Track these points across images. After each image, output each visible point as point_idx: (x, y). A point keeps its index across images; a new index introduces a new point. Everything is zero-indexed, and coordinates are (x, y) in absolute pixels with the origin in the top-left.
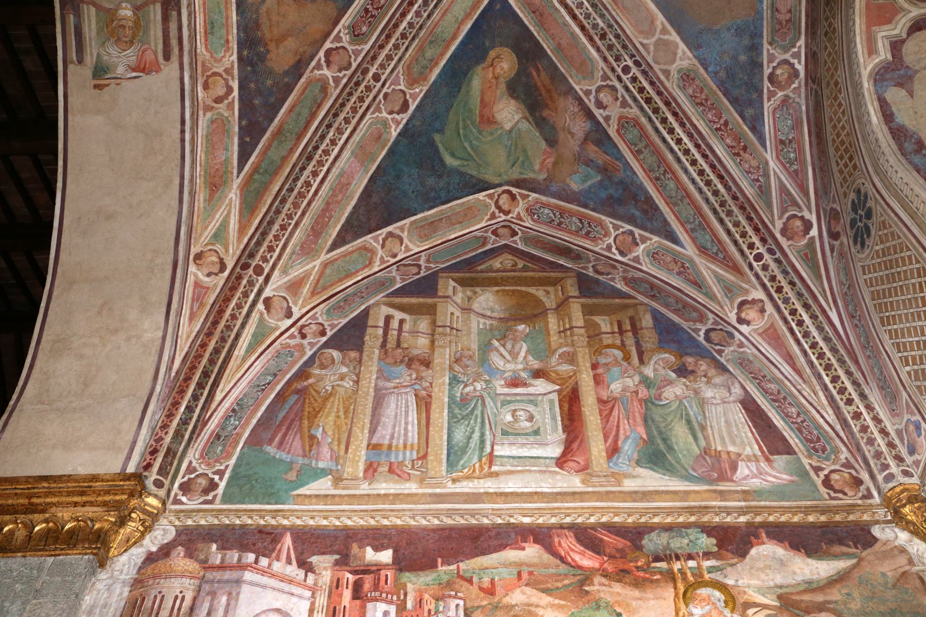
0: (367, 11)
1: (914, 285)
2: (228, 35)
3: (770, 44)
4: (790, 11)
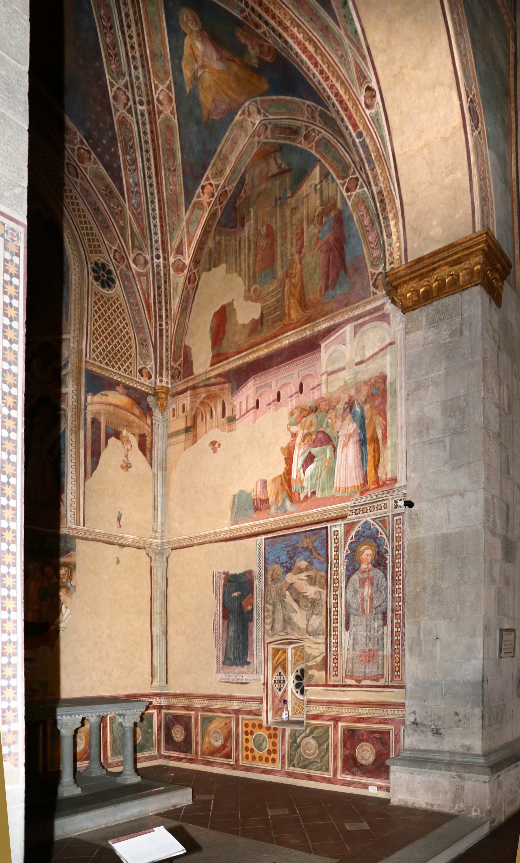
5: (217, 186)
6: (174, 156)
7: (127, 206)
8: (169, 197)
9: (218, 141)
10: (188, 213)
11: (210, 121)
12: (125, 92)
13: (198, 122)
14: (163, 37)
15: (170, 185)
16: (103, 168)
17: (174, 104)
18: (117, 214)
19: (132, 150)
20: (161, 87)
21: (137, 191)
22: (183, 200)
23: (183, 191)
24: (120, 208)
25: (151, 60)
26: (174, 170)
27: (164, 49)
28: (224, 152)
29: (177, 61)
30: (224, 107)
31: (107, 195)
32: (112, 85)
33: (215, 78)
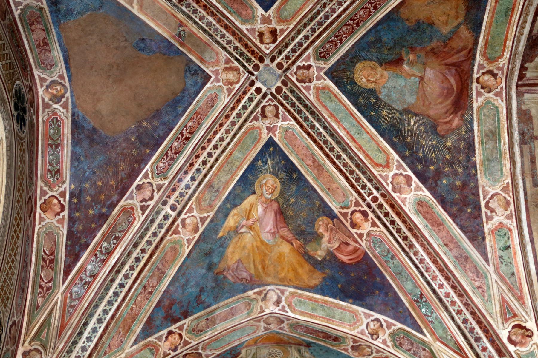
0: (375, 8)
2: (495, 6)
3: (42, 8)
4: (33, 31)
5: (186, 343)
6: (160, 280)
7: (62, 288)
8: (125, 314)
9: (217, 299)
10: (134, 347)
11: (222, 276)
12: (153, 191)
13: (210, 268)
14: (231, 180)
15: (135, 304)
16: (65, 232)
17: (197, 236)
18: (41, 287)
19: (115, 241)
20: (195, 213)
21: (89, 282)
22: (139, 330)
23: (145, 320)
24: (50, 285)
25: (204, 187)
26: (151, 293)
27: (224, 188)
28: (215, 314)
29: (228, 206)
30: (245, 275)
31: (44, 260)
32: (146, 176)
33: (255, 244)
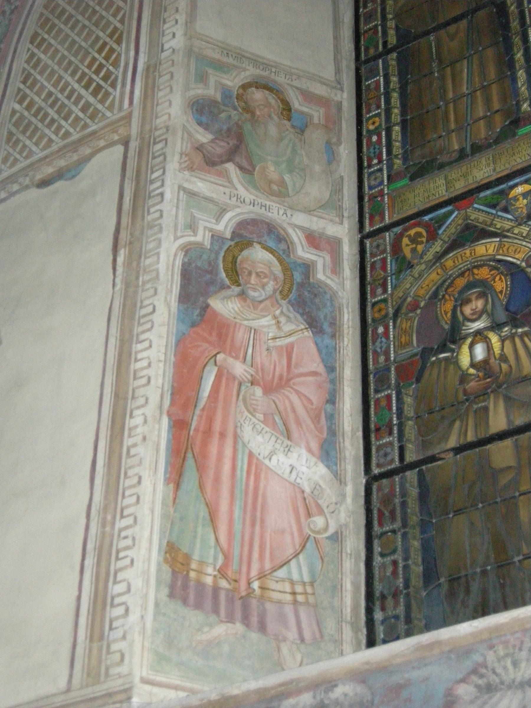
1: (98, 38)
